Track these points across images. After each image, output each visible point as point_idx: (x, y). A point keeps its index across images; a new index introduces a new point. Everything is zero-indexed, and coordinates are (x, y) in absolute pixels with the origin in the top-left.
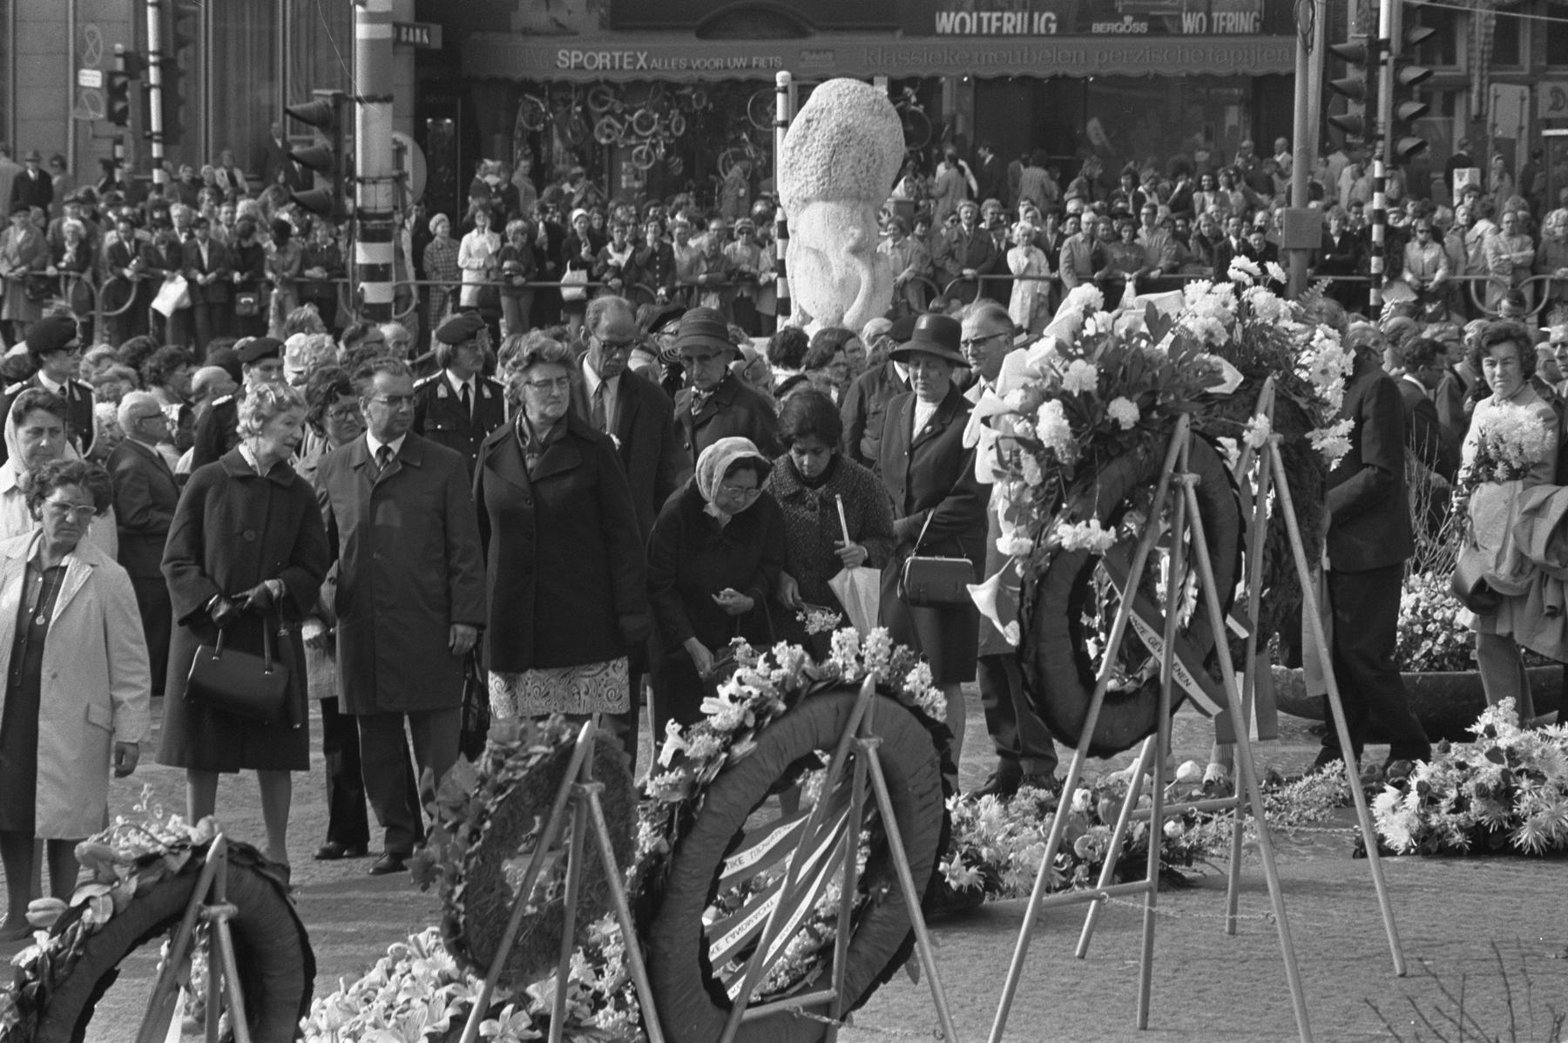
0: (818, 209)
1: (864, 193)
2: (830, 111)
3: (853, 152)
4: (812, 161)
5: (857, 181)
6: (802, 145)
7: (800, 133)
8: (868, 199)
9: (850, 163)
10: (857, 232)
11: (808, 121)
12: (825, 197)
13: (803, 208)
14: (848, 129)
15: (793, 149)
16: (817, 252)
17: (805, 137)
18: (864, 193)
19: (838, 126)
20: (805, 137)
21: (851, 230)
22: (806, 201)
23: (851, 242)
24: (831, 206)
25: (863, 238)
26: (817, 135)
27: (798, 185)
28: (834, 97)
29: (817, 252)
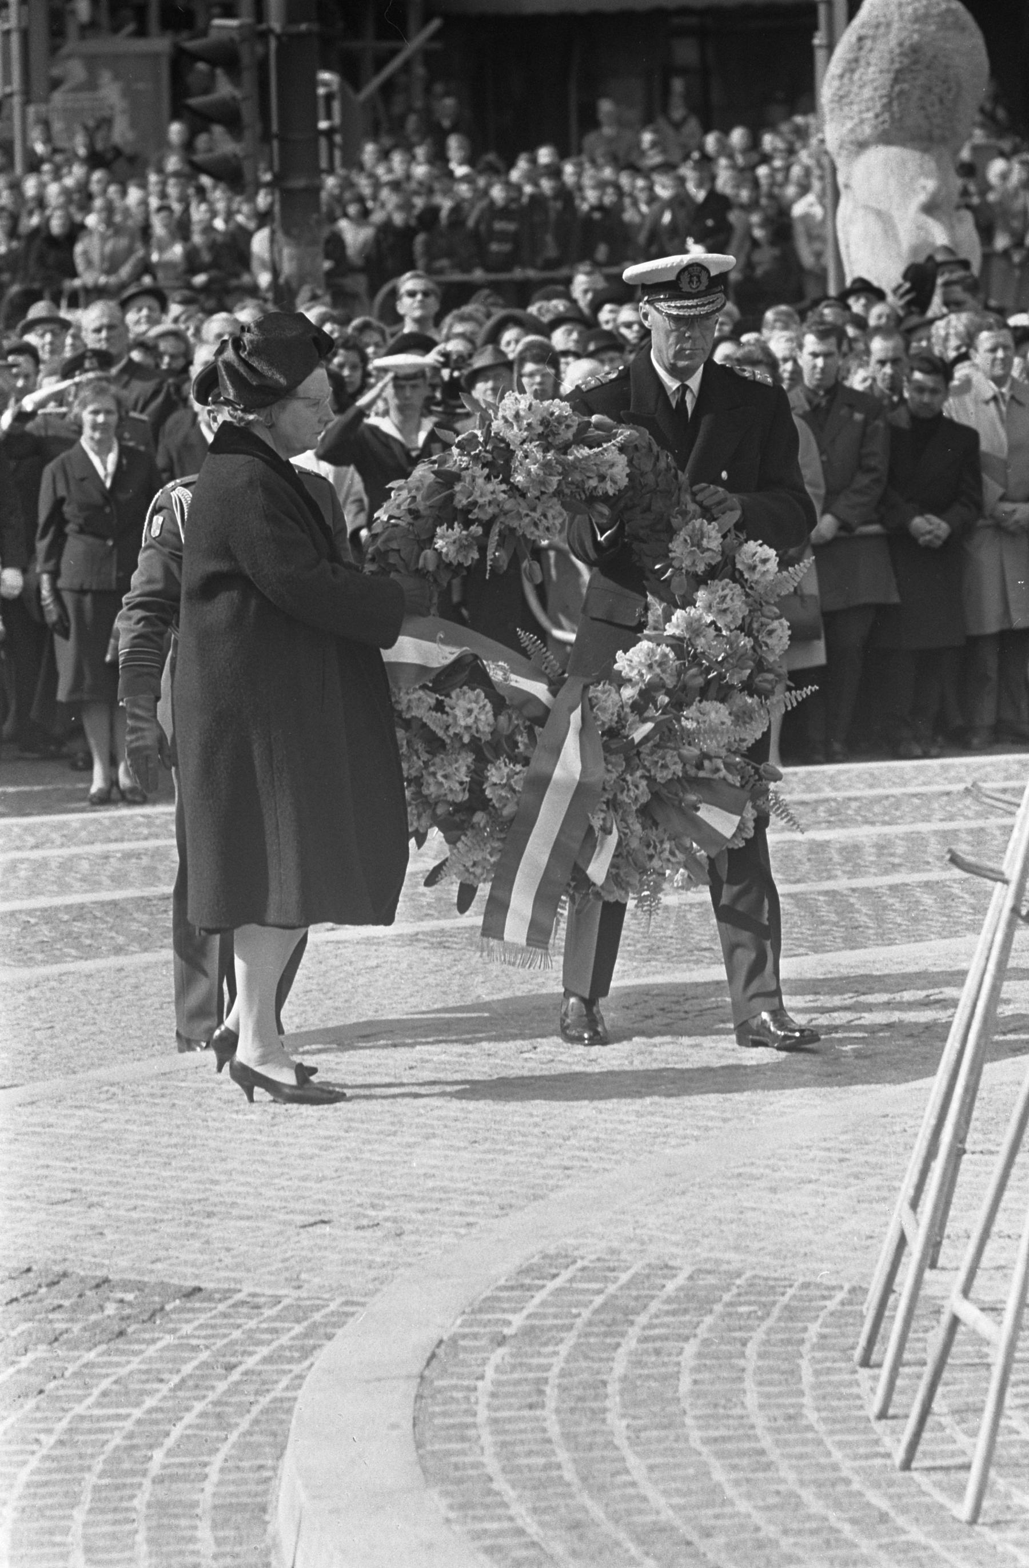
0: (878, 156)
1: (937, 132)
2: (888, 25)
3: (921, 80)
4: (867, 93)
5: (927, 117)
6: (852, 71)
7: (851, 56)
8: (943, 140)
9: (917, 93)
10: (931, 184)
11: (860, 39)
12: (885, 138)
13: (858, 154)
14: (915, 49)
15: (841, 76)
16: (879, 214)
17: (856, 60)
19: (901, 44)
20: (856, 60)
22: (862, 146)
23: (922, 198)
24: (894, 151)
25: (939, 190)
26: (874, 58)
27: (849, 125)
28: (893, 8)
29: (879, 214)
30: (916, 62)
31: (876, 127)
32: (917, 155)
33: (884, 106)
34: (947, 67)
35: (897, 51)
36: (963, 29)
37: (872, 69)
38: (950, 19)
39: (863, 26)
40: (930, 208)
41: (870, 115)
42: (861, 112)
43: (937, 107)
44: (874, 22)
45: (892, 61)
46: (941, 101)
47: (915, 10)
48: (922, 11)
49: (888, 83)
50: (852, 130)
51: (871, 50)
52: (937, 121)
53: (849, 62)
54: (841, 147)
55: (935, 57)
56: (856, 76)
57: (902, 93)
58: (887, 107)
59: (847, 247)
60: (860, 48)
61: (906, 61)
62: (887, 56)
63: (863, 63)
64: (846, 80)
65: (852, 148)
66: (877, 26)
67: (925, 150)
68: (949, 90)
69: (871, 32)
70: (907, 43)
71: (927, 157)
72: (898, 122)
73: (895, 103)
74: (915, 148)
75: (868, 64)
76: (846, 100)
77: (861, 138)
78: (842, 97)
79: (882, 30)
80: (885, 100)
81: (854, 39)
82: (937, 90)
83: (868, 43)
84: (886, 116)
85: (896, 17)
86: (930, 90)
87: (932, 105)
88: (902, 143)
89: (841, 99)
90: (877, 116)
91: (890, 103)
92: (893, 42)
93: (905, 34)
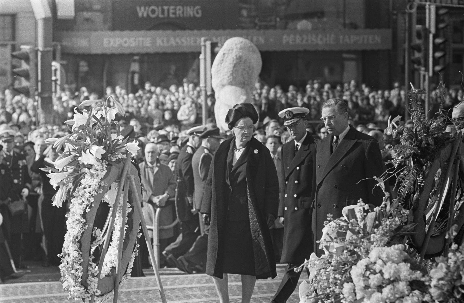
1: (246, 82)
2: (233, 50)
5: (243, 78)
6: (221, 64)
7: (221, 59)
8: (248, 84)
11: (224, 54)
12: (231, 84)
13: (222, 88)
14: (240, 57)
15: (218, 65)
17: (223, 60)
19: (236, 56)
20: (223, 60)
22: (223, 86)
24: (233, 87)
27: (220, 79)
28: (234, 45)
30: (241, 61)
31: (228, 81)
32: (240, 89)
34: (250, 63)
35: (235, 58)
36: (255, 52)
37: (227, 63)
38: (251, 49)
39: (225, 50)
41: (227, 76)
42: (223, 76)
43: (246, 75)
44: (228, 49)
45: (234, 61)
46: (248, 73)
47: (241, 46)
48: (242, 46)
49: (232, 68)
50: (221, 81)
51: (227, 57)
52: (247, 79)
53: (221, 61)
54: (217, 86)
55: (246, 60)
56: (223, 65)
57: (236, 70)
58: (232, 74)
59: (218, 116)
60: (224, 57)
61: (238, 61)
62: (232, 60)
63: (224, 61)
64: (219, 66)
65: (221, 86)
66: (229, 50)
67: (243, 88)
68: (250, 70)
69: (227, 52)
70: (238, 56)
71: (243, 89)
72: (234, 78)
74: (240, 87)
75: (226, 62)
77: (223, 84)
78: (218, 71)
79: (231, 51)
80: (231, 72)
81: (222, 54)
82: (247, 69)
83: (226, 56)
84: (231, 77)
85: (235, 48)
86: (244, 70)
87: (245, 74)
88: (236, 85)
89: (218, 71)
90: (228, 77)
92: (234, 55)
93: (237, 53)
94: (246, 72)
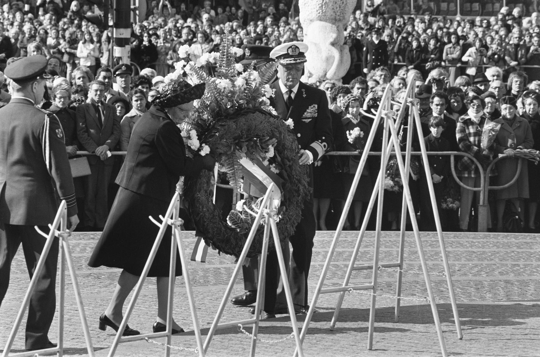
1: (338, 18)
5: (334, 12)
8: (340, 20)
10: (334, 35)
18: (338, 18)
21: (331, 34)
23: (332, 40)
29: (315, 44)
32: (330, 25)
33: (320, 7)
40: (333, 44)
41: (315, 10)
52: (338, 14)
67: (333, 24)
72: (324, 13)
73: (324, 7)
76: (307, 5)
77: (311, 18)
80: (320, 5)
88: (326, 21)
90: (317, 11)
91: (322, 6)
94: (338, 6)
